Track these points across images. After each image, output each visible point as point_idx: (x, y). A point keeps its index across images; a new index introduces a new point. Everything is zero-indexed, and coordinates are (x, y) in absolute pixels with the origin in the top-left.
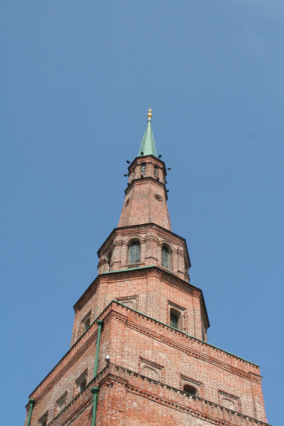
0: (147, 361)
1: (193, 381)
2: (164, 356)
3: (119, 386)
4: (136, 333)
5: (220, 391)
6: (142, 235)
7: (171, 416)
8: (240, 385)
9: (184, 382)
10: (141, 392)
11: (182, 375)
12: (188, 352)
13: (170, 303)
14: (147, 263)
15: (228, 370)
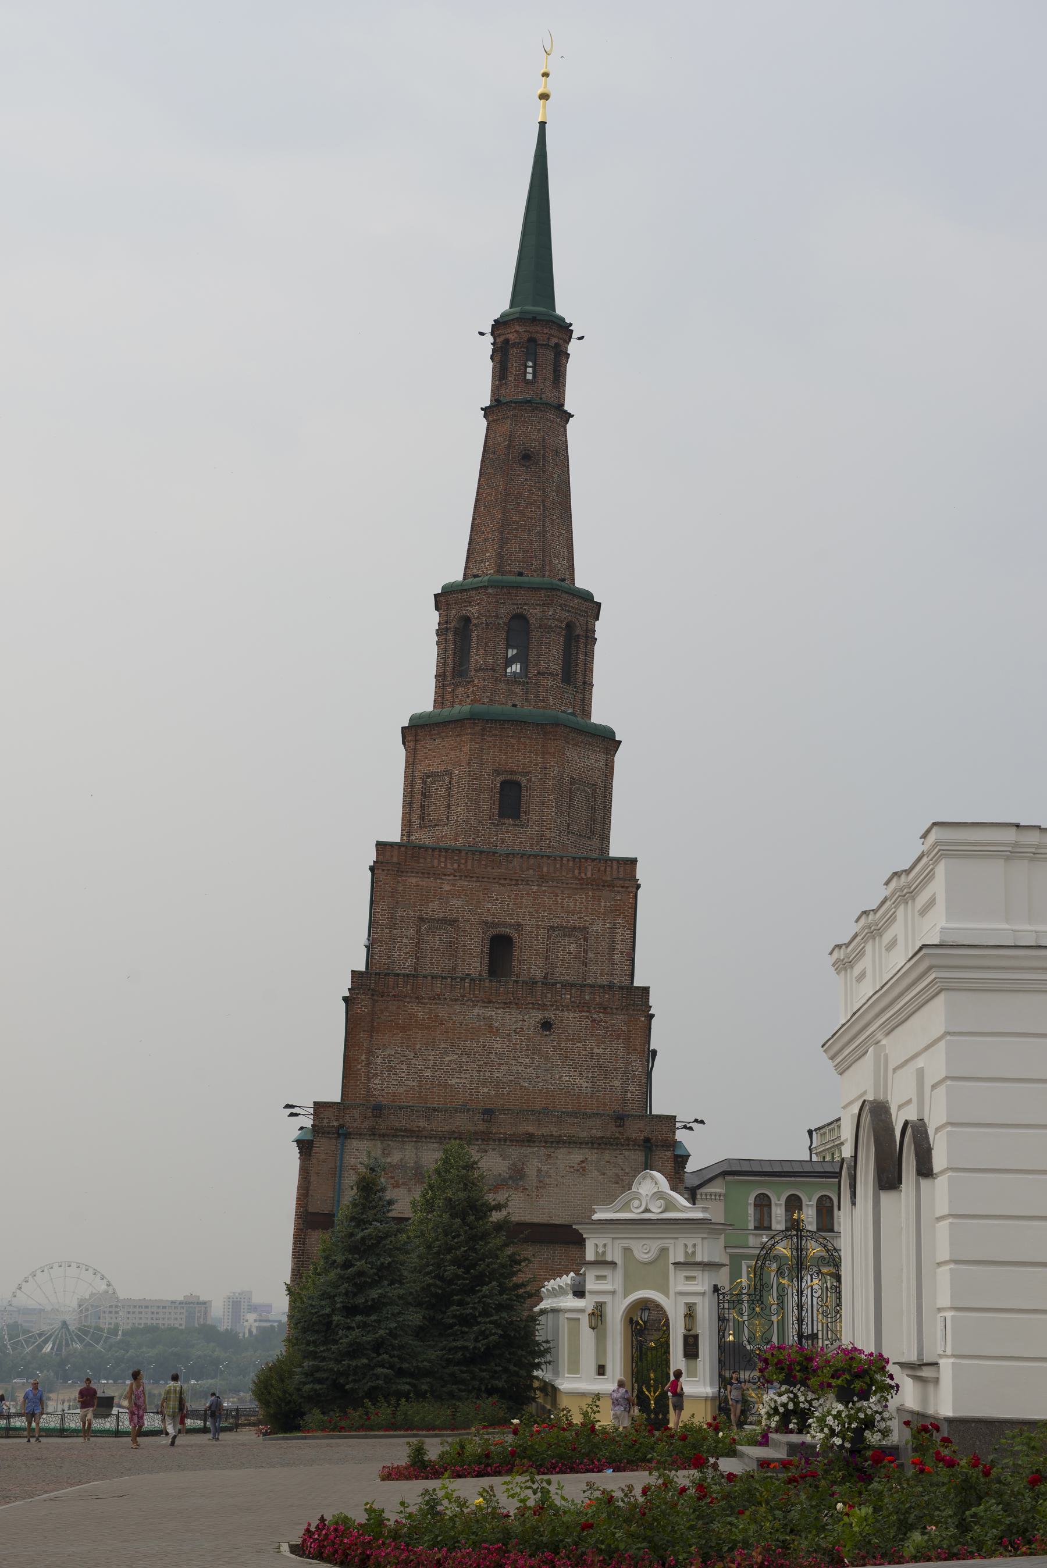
0: (431, 920)
1: (505, 925)
2: (457, 903)
3: (362, 1000)
4: (414, 881)
5: (552, 927)
6: (473, 610)
7: (437, 1016)
8: (593, 904)
9: (492, 932)
10: (394, 996)
11: (486, 923)
12: (502, 881)
13: (497, 772)
14: (476, 681)
15: (574, 886)
